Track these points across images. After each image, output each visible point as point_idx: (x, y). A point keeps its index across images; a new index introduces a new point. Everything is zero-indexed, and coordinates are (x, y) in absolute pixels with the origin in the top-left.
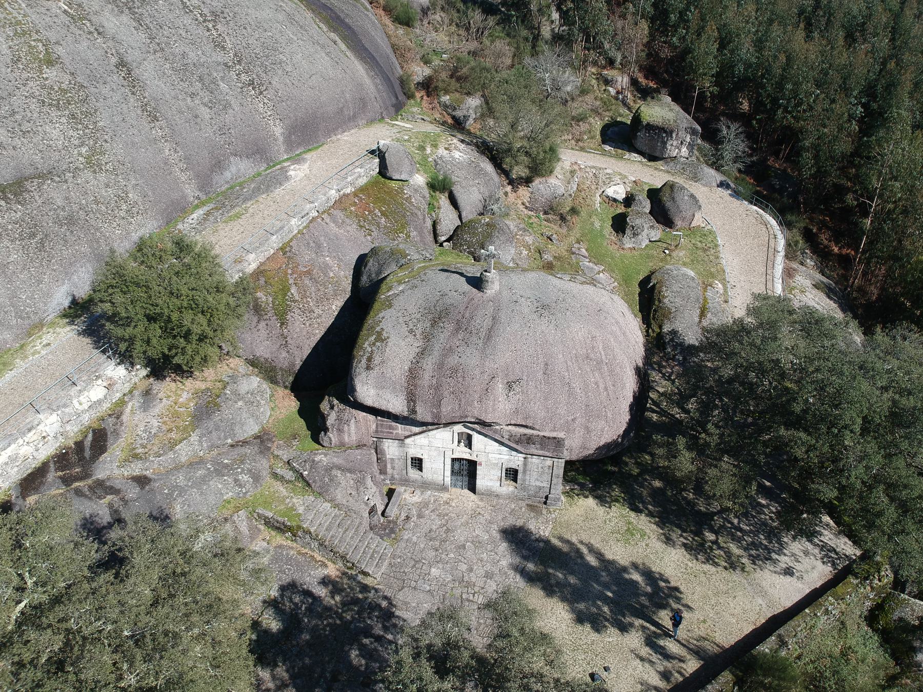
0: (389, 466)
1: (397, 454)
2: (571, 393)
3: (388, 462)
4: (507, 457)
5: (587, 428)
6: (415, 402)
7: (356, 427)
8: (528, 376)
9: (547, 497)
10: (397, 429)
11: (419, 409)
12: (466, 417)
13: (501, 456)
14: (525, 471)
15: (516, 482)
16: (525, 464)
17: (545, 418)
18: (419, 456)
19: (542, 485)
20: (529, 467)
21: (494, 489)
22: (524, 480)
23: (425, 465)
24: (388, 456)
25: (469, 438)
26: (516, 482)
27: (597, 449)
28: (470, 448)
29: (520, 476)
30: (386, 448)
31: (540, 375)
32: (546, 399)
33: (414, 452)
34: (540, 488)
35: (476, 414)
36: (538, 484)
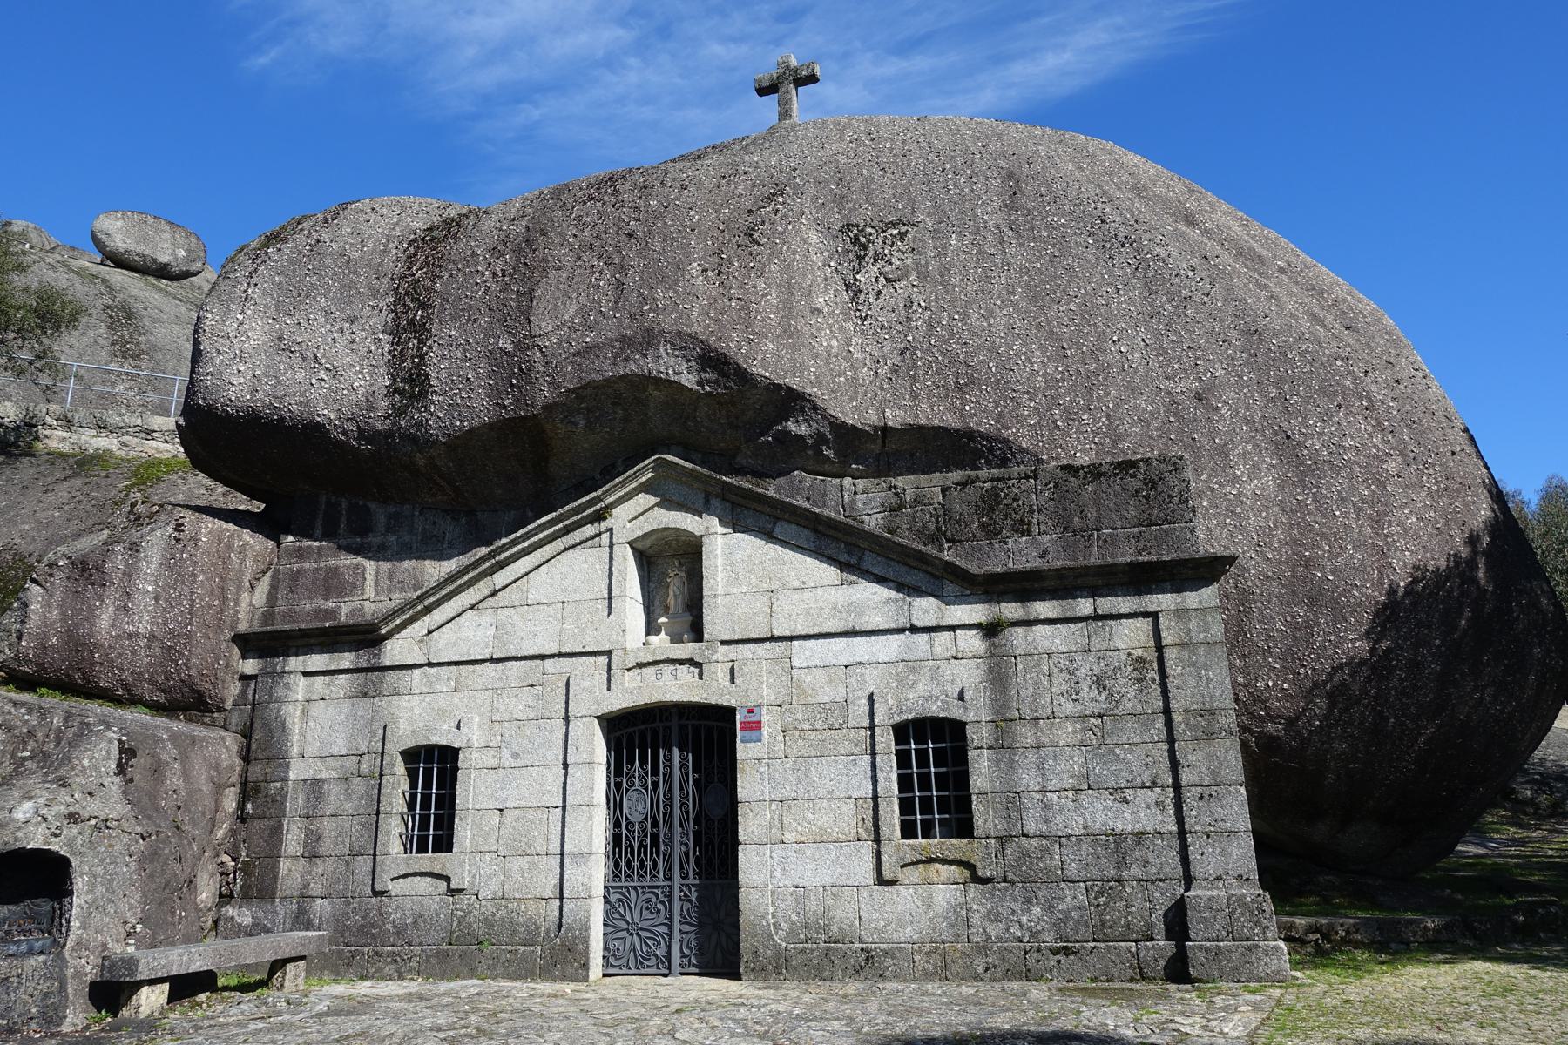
0: (293, 840)
1: (340, 747)
2: (1150, 274)
3: (295, 803)
4: (892, 646)
5: (1286, 446)
6: (420, 330)
7: (170, 564)
8: (937, 209)
9: (1177, 921)
10: (356, 587)
11: (439, 368)
12: (649, 339)
13: (861, 648)
14: (1003, 724)
15: (964, 828)
16: (999, 678)
17: (1052, 383)
18: (442, 736)
19: (1126, 819)
20: (1023, 695)
21: (844, 914)
22: (1012, 800)
23: (474, 793)
24: (297, 772)
25: (690, 553)
26: (964, 828)
27: (1393, 614)
28: (698, 637)
29: (982, 771)
30: (292, 714)
31: (990, 215)
32: (1034, 297)
33: (418, 714)
34: (1121, 845)
35: (696, 319)
36: (1102, 814)
